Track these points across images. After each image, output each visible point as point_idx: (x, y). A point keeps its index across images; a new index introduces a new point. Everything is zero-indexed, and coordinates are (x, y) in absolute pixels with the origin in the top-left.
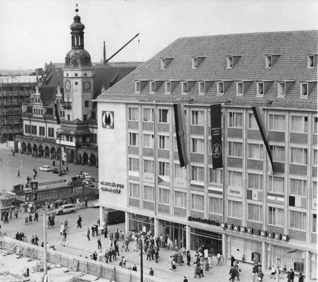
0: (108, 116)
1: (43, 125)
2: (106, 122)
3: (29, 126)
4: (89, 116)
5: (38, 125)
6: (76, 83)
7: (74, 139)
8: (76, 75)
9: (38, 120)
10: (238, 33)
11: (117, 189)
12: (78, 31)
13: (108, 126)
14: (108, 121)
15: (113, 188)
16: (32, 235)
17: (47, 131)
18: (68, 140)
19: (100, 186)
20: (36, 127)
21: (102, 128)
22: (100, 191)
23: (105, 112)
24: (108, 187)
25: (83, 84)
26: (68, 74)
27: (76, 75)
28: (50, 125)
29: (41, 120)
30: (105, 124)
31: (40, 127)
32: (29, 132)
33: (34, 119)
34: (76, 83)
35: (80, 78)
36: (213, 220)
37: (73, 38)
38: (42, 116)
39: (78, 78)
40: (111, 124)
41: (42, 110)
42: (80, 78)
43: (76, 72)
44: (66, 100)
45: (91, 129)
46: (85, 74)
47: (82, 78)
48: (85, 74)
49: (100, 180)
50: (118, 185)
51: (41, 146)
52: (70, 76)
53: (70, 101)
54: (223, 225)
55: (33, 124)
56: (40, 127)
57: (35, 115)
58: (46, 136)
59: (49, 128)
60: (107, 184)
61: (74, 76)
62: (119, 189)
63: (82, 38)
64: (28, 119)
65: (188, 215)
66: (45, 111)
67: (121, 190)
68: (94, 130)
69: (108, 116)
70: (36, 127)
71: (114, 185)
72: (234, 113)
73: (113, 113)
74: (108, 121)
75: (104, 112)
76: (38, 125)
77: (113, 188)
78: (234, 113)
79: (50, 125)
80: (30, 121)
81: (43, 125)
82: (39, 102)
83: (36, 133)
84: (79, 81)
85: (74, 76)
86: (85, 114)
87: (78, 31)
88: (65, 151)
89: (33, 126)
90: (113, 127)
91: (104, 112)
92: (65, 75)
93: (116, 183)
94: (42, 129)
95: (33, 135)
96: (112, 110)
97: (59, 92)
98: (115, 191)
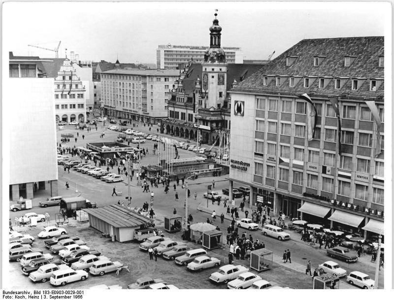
0: (239, 105)
1: (184, 111)
3: (173, 112)
4: (222, 105)
5: (180, 111)
6: (213, 77)
7: (209, 124)
8: (213, 69)
9: (180, 107)
11: (243, 167)
12: (216, 33)
13: (239, 114)
14: (239, 109)
15: (241, 166)
17: (187, 116)
18: (204, 124)
20: (178, 112)
23: (237, 101)
24: (237, 165)
25: (219, 78)
26: (206, 69)
27: (213, 69)
29: (183, 107)
30: (236, 112)
31: (182, 113)
32: (173, 117)
33: (177, 106)
34: (213, 77)
36: (325, 196)
37: (211, 38)
38: (183, 104)
40: (242, 112)
41: (184, 99)
44: (203, 91)
45: (223, 116)
48: (221, 69)
50: (245, 164)
51: (182, 129)
52: (207, 70)
53: (207, 91)
54: (333, 201)
55: (177, 110)
56: (182, 113)
57: (177, 103)
59: (189, 114)
60: (237, 162)
61: (211, 71)
63: (219, 38)
64: (172, 105)
65: (304, 191)
66: (186, 99)
67: (248, 168)
68: (226, 117)
69: (239, 105)
70: (178, 112)
71: (241, 163)
73: (243, 103)
74: (239, 109)
75: (236, 102)
76: (180, 111)
77: (241, 166)
80: (174, 107)
81: (184, 111)
82: (181, 92)
83: (178, 118)
84: (216, 75)
85: (211, 71)
86: (219, 103)
87: (216, 33)
88: (201, 134)
89: (176, 112)
90: (243, 115)
91: (236, 102)
92: (204, 70)
93: (243, 162)
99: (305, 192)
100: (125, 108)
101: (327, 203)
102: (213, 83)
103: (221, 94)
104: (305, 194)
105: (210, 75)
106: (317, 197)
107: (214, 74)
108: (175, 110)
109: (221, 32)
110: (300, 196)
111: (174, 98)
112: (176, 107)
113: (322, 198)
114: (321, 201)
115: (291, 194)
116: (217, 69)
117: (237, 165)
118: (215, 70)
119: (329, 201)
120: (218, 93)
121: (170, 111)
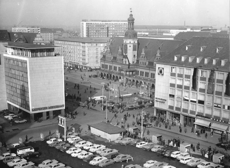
0: (161, 70)
1: (111, 65)
2: (160, 72)
4: (135, 62)
5: (108, 64)
8: (130, 42)
9: (108, 62)
10: (170, 25)
14: (161, 72)
15: (161, 101)
16: (205, 149)
17: (113, 68)
19: (155, 99)
21: (158, 75)
22: (155, 101)
26: (126, 42)
27: (130, 42)
28: (114, 65)
29: (110, 62)
30: (159, 73)
31: (110, 66)
32: (104, 68)
33: (106, 62)
34: (130, 46)
35: (132, 44)
39: (131, 44)
40: (162, 73)
41: (111, 58)
42: (132, 44)
43: (130, 41)
44: (124, 54)
45: (136, 68)
46: (134, 42)
47: (133, 44)
48: (134, 42)
49: (156, 97)
50: (164, 100)
51: (111, 75)
52: (127, 43)
53: (127, 54)
54: (212, 119)
56: (110, 66)
58: (113, 70)
59: (114, 67)
60: (159, 99)
61: (129, 43)
62: (164, 101)
64: (103, 61)
65: (196, 114)
66: (112, 58)
67: (165, 101)
68: (138, 69)
69: (161, 70)
70: (107, 65)
71: (162, 99)
72: (203, 71)
73: (163, 68)
74: (161, 72)
75: (159, 68)
76: (108, 64)
78: (203, 71)
79: (114, 65)
81: (111, 65)
82: (109, 53)
84: (132, 45)
85: (129, 43)
86: (133, 61)
89: (106, 65)
90: (163, 75)
91: (159, 68)
92: (124, 42)
94: (110, 67)
95: (106, 69)
96: (163, 67)
97: (120, 49)
98: (162, 102)
99: (197, 114)
100: (71, 61)
101: (208, 119)
102: (130, 50)
103: (134, 56)
104: (197, 115)
105: (128, 45)
106: (204, 117)
107: (131, 45)
108: (105, 64)
109: (134, 21)
110: (194, 116)
111: (104, 56)
112: (106, 62)
113: (206, 117)
114: (206, 119)
115: (189, 115)
116: (132, 42)
117: (159, 100)
118: (131, 43)
119: (209, 118)
120: (133, 55)
121: (102, 64)
